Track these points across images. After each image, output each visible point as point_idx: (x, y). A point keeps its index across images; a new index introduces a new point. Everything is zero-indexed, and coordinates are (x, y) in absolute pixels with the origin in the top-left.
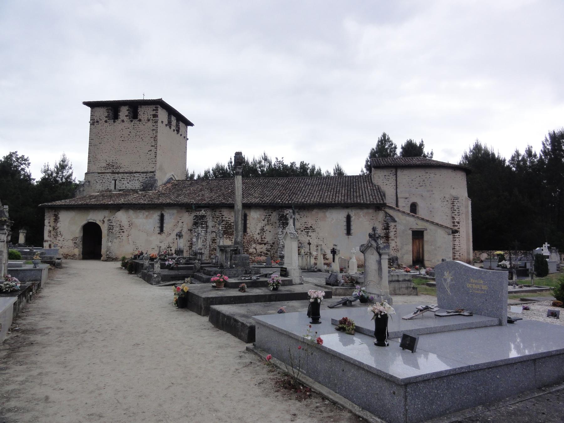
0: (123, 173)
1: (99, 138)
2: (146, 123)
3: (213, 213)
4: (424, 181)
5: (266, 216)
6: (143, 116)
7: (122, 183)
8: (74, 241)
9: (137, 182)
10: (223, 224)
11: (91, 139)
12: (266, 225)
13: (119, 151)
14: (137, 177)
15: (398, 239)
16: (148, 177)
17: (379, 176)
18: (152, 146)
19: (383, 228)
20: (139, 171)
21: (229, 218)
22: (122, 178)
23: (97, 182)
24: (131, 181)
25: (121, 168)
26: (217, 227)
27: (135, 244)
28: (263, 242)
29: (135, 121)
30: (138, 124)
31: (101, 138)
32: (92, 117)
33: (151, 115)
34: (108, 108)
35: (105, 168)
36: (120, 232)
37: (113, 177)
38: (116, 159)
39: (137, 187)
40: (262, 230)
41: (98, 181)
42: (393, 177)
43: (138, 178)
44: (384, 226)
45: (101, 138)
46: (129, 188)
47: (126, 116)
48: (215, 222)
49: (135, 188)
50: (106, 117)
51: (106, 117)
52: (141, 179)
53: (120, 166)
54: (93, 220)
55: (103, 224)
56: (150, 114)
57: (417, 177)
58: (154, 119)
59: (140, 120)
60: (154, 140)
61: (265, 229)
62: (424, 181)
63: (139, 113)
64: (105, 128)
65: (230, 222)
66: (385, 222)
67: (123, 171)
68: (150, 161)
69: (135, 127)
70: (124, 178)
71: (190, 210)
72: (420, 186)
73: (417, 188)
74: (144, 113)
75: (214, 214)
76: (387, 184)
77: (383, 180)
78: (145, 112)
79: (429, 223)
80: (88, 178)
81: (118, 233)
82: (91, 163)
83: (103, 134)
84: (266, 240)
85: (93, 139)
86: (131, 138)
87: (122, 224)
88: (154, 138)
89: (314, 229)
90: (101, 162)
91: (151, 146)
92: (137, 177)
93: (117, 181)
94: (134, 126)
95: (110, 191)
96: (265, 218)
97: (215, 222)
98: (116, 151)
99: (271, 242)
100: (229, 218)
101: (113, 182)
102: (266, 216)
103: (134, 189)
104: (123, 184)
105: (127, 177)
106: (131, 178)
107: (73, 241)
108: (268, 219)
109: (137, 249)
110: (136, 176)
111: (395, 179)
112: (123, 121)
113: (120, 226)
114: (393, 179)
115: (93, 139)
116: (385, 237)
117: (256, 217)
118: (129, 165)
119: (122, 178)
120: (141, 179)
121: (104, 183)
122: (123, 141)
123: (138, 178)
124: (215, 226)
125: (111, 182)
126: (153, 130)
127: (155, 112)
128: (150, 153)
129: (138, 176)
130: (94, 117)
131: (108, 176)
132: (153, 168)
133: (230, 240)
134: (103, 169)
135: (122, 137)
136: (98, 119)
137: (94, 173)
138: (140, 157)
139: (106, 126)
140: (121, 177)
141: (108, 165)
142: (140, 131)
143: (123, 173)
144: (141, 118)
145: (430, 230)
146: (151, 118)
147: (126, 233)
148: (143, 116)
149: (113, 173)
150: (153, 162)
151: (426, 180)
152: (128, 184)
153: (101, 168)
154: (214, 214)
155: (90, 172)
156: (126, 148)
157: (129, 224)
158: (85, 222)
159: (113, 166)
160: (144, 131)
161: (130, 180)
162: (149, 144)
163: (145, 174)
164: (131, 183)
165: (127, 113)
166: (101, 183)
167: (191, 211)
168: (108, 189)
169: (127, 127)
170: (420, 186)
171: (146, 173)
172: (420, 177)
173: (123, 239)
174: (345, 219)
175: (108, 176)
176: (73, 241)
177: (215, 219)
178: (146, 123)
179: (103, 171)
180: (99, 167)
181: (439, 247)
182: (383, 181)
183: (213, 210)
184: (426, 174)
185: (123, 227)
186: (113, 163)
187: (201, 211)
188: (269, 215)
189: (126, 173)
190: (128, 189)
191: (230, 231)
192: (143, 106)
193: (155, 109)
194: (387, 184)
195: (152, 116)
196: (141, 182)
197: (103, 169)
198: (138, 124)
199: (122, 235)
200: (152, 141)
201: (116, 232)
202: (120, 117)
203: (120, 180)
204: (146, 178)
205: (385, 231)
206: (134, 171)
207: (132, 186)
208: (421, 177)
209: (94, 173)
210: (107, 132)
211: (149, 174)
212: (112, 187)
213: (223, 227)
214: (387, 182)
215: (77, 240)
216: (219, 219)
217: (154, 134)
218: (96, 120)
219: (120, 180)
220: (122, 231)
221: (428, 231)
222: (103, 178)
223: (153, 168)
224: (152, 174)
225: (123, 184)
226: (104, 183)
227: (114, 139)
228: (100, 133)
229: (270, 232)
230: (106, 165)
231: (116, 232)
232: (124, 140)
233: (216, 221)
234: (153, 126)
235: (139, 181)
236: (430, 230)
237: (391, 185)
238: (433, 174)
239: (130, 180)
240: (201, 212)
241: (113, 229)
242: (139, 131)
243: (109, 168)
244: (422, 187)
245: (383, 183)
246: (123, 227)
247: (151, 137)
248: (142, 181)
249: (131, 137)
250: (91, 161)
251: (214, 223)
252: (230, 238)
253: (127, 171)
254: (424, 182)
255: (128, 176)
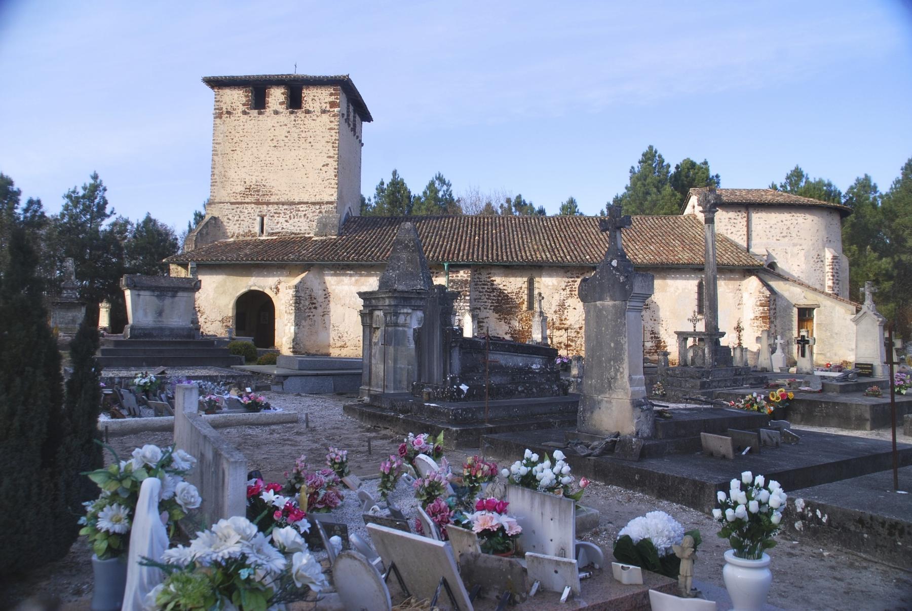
0: (277, 203)
1: (230, 141)
2: (317, 116)
3: (476, 277)
4: (788, 228)
5: (569, 282)
6: (311, 105)
7: (276, 221)
8: (225, 324)
9: (302, 219)
10: (494, 296)
11: (217, 143)
12: (567, 298)
13: (269, 165)
14: (303, 211)
15: (777, 321)
16: (323, 211)
17: (720, 219)
18: (330, 157)
19: (758, 304)
20: (305, 200)
21: (504, 286)
22: (275, 213)
23: (228, 219)
24: (292, 217)
25: (271, 195)
26: (484, 301)
27: (337, 328)
28: (563, 326)
29: (300, 113)
30: (303, 118)
31: (235, 141)
32: (218, 104)
33: (326, 103)
34: (248, 89)
35: (244, 195)
36: (310, 308)
37: (258, 210)
38: (264, 179)
39: (303, 228)
40: (562, 306)
41: (231, 218)
42: (741, 220)
43: (304, 213)
44: (760, 300)
45: (235, 141)
46: (289, 231)
47: (281, 103)
48: (480, 292)
49: (300, 230)
50: (244, 105)
51: (244, 105)
52: (311, 214)
53: (270, 192)
54: (259, 287)
55: (276, 293)
56: (326, 101)
57: (777, 222)
58: (332, 110)
59: (308, 112)
60: (333, 147)
61: (567, 305)
62: (788, 228)
63: (305, 99)
64: (242, 124)
65: (506, 292)
66: (761, 295)
67: (276, 201)
68: (326, 183)
69: (297, 122)
70: (280, 213)
71: (435, 271)
72: (784, 237)
73: (778, 240)
74: (313, 99)
75: (478, 278)
76: (732, 233)
77: (726, 225)
78: (315, 98)
79: (823, 296)
80: (214, 213)
81: (307, 310)
82: (217, 186)
83: (237, 135)
84: (568, 323)
85: (219, 143)
86: (290, 142)
87: (313, 294)
88: (333, 143)
89: (647, 305)
90: (235, 184)
91: (328, 157)
92: (303, 211)
93: (265, 219)
94: (295, 121)
95: (254, 235)
96: (566, 286)
97: (480, 292)
98: (263, 165)
99: (577, 326)
100: (504, 286)
101: (258, 219)
102: (569, 282)
103: (298, 231)
104: (278, 223)
105: (286, 211)
106: (291, 212)
107: (223, 323)
108: (572, 288)
109: (339, 337)
110: (301, 209)
111: (745, 224)
112: (276, 112)
113: (311, 298)
114: (741, 224)
115: (219, 143)
116: (760, 317)
117: (550, 284)
118: (288, 190)
119: (275, 213)
120: (310, 215)
121: (243, 220)
122: (275, 146)
123: (304, 213)
124: (480, 299)
125: (255, 219)
126: (331, 129)
127: (333, 97)
128: (324, 169)
129: (304, 209)
130: (222, 104)
131: (250, 209)
132: (332, 195)
133: (506, 323)
134: (238, 197)
135: (273, 140)
136: (229, 108)
137: (223, 203)
138: (307, 176)
139: (244, 121)
140: (273, 210)
141: (249, 189)
142: (307, 130)
143: (277, 203)
144: (308, 108)
145: (825, 306)
146: (326, 107)
147: (320, 310)
148: (311, 105)
149: (258, 203)
150: (331, 186)
151: (792, 227)
152: (288, 224)
153: (234, 194)
154: (478, 278)
155: (216, 201)
156: (281, 160)
157: (325, 295)
158: (243, 290)
159: (258, 191)
160: (313, 130)
161: (290, 216)
162: (323, 154)
163: (318, 207)
164: (291, 222)
165: (282, 98)
166: (238, 220)
167: (437, 273)
168: (250, 231)
169: (282, 124)
170: (784, 237)
171: (320, 204)
172: (782, 221)
173: (315, 321)
174: (696, 289)
175: (250, 209)
176: (223, 323)
177: (480, 287)
178: (317, 116)
179: (240, 200)
180: (232, 192)
181: (837, 334)
182: (727, 228)
183: (476, 271)
184: (791, 218)
185: (315, 299)
186: (257, 185)
187: (458, 272)
188: (573, 281)
189: (283, 204)
190: (287, 232)
191: (507, 308)
192: (311, 88)
193: (334, 92)
194: (732, 233)
195: (328, 105)
196: (311, 221)
197: (238, 197)
198: (303, 118)
199: (313, 314)
200: (328, 148)
201: (305, 308)
202: (269, 105)
203: (272, 216)
204: (320, 212)
205: (761, 308)
206: (297, 200)
207: (294, 226)
208: (785, 222)
209: (223, 203)
210: (245, 131)
211: (325, 206)
212: (257, 229)
213: (493, 299)
214: (733, 230)
215: (229, 321)
216: (486, 287)
217: (332, 136)
218: (224, 110)
219: (272, 216)
220: (314, 305)
221: (822, 308)
222: (241, 212)
223: (332, 195)
224: (331, 206)
225: (278, 223)
226: (243, 220)
227: (260, 145)
228: (233, 132)
229: (575, 309)
230: (244, 190)
231: (305, 308)
232: (277, 145)
233: (481, 290)
234: (331, 122)
235: (308, 217)
236: (825, 306)
237: (739, 233)
238: (802, 218)
239: (290, 216)
240: (459, 275)
241: (300, 303)
242: (304, 130)
243: (251, 194)
244: (786, 239)
245: (727, 230)
246: (315, 299)
247: (327, 142)
248: (312, 219)
249: (289, 140)
250: (216, 182)
251: (477, 293)
252: (506, 318)
253: (283, 200)
254: (788, 231)
255: (286, 209)
